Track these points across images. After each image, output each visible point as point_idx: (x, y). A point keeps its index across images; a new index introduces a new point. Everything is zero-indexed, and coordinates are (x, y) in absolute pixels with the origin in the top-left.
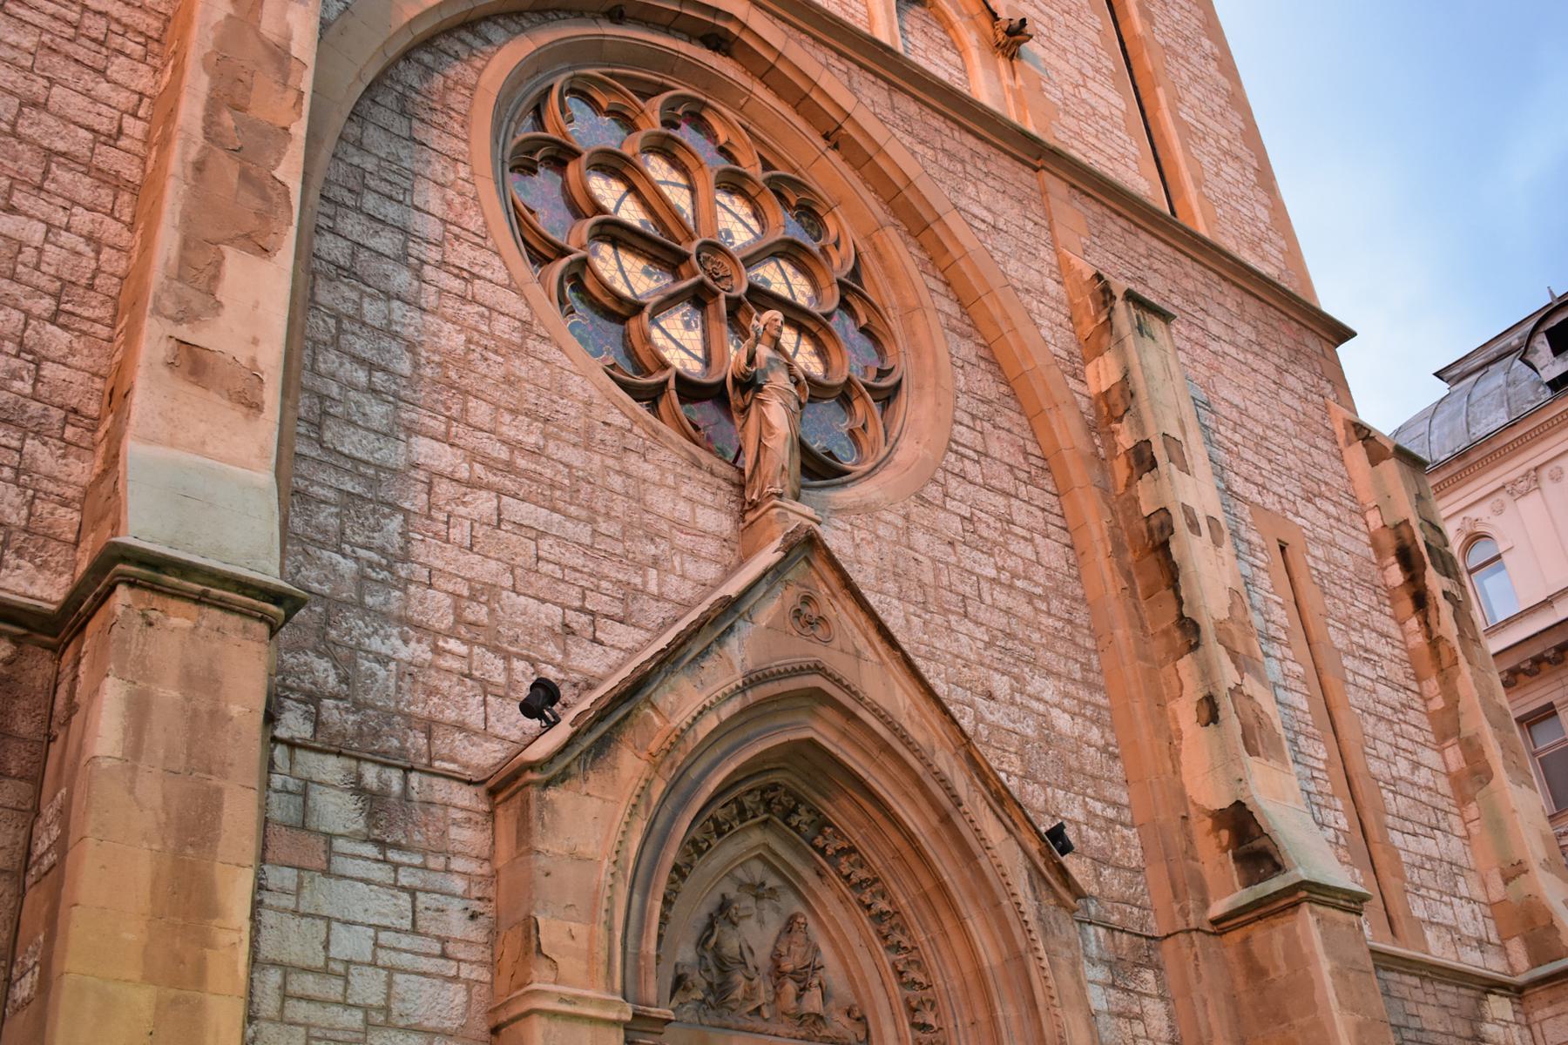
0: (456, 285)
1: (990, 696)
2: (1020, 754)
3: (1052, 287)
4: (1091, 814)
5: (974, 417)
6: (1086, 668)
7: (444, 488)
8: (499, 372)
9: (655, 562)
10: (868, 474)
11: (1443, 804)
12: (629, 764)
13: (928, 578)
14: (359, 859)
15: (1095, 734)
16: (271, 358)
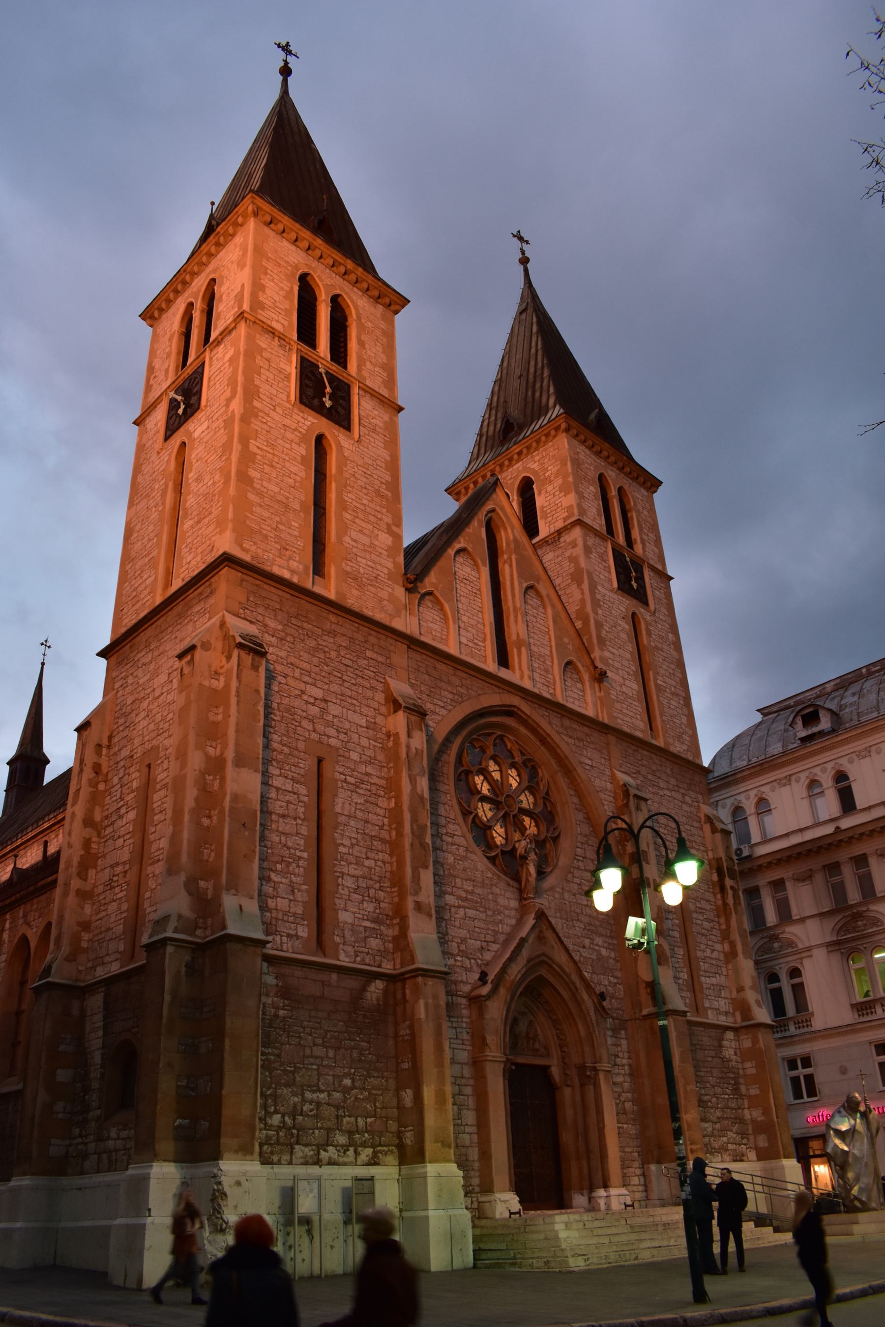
1: (584, 947)
3: (609, 786)
4: (610, 982)
5: (582, 843)
6: (611, 931)
7: (453, 910)
8: (462, 867)
9: (501, 922)
10: (551, 871)
11: (720, 964)
12: (502, 991)
13: (568, 909)
15: (613, 955)
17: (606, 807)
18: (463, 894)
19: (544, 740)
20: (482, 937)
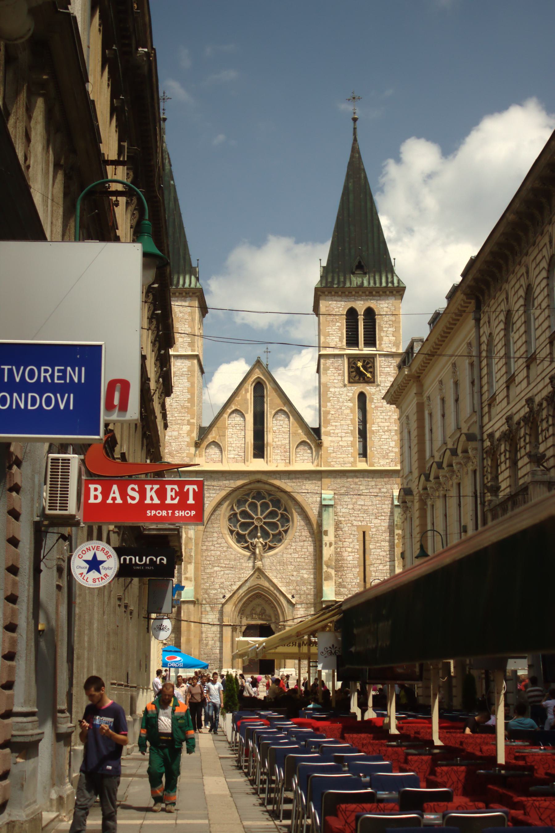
0: (219, 545)
2: (296, 583)
4: (307, 588)
13: (285, 561)
14: (211, 613)
16: (193, 576)
17: (315, 511)
18: (224, 566)
19: (278, 488)
20: (232, 580)
